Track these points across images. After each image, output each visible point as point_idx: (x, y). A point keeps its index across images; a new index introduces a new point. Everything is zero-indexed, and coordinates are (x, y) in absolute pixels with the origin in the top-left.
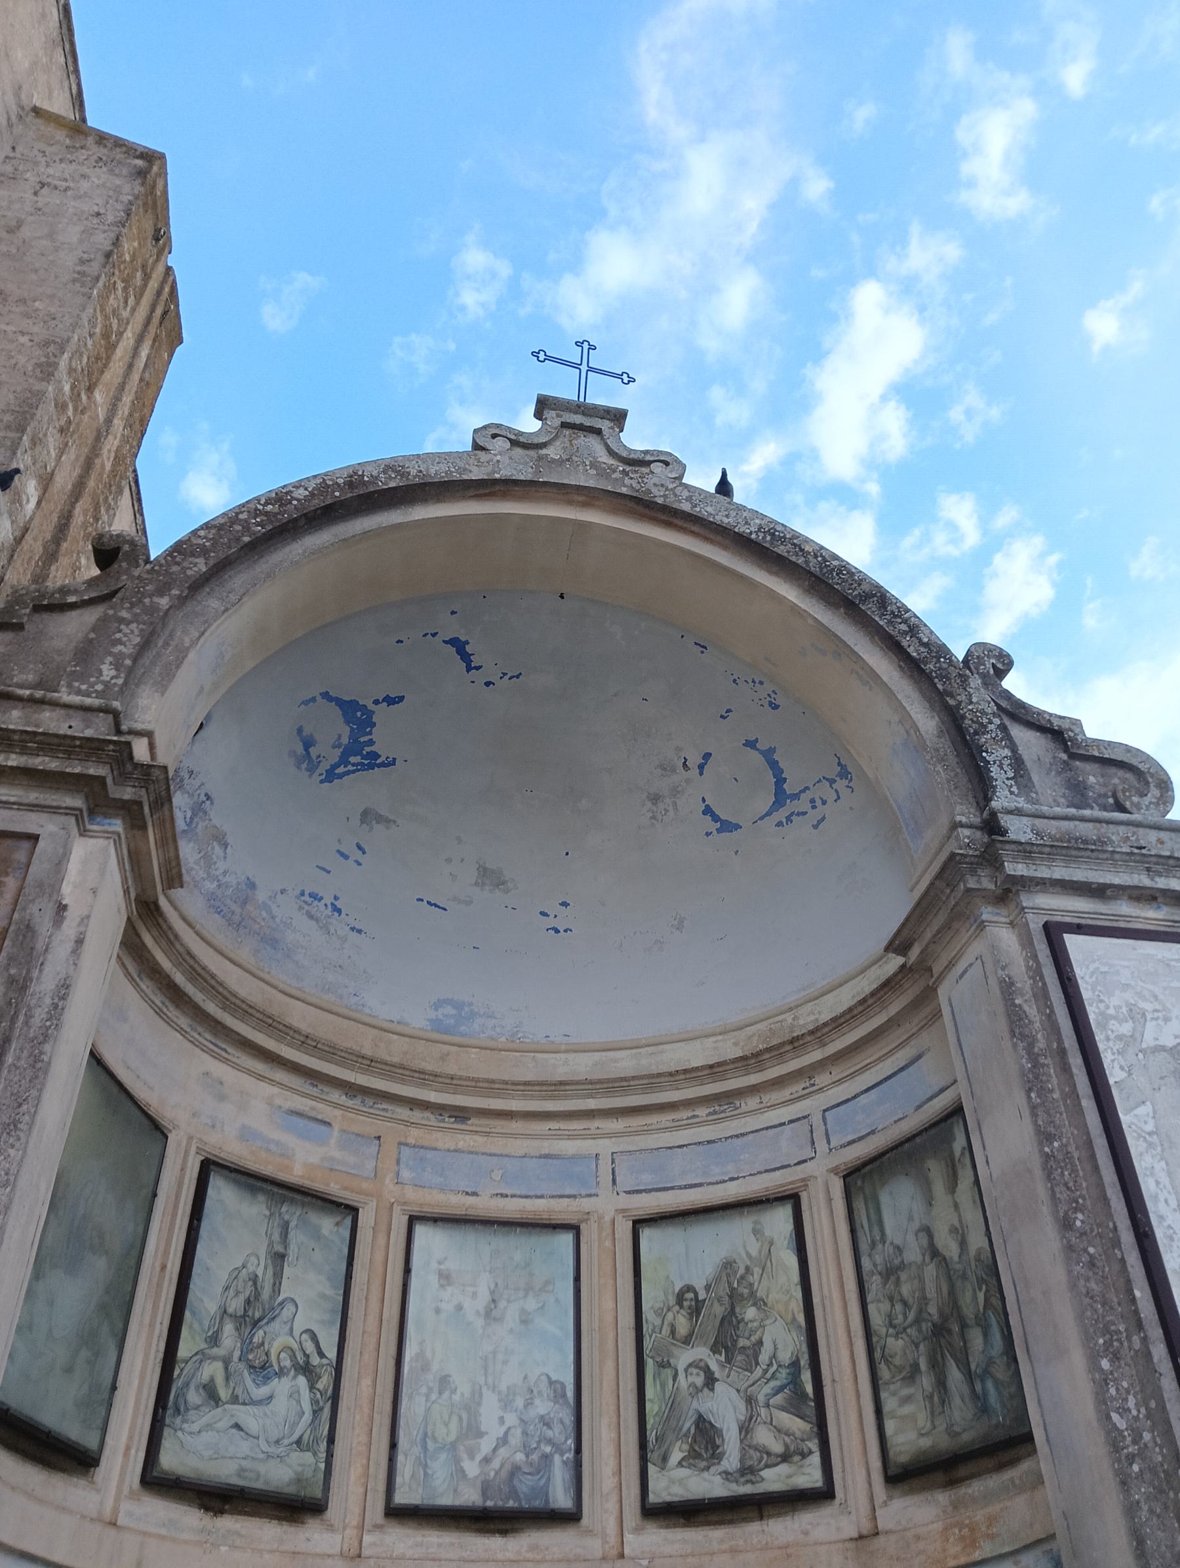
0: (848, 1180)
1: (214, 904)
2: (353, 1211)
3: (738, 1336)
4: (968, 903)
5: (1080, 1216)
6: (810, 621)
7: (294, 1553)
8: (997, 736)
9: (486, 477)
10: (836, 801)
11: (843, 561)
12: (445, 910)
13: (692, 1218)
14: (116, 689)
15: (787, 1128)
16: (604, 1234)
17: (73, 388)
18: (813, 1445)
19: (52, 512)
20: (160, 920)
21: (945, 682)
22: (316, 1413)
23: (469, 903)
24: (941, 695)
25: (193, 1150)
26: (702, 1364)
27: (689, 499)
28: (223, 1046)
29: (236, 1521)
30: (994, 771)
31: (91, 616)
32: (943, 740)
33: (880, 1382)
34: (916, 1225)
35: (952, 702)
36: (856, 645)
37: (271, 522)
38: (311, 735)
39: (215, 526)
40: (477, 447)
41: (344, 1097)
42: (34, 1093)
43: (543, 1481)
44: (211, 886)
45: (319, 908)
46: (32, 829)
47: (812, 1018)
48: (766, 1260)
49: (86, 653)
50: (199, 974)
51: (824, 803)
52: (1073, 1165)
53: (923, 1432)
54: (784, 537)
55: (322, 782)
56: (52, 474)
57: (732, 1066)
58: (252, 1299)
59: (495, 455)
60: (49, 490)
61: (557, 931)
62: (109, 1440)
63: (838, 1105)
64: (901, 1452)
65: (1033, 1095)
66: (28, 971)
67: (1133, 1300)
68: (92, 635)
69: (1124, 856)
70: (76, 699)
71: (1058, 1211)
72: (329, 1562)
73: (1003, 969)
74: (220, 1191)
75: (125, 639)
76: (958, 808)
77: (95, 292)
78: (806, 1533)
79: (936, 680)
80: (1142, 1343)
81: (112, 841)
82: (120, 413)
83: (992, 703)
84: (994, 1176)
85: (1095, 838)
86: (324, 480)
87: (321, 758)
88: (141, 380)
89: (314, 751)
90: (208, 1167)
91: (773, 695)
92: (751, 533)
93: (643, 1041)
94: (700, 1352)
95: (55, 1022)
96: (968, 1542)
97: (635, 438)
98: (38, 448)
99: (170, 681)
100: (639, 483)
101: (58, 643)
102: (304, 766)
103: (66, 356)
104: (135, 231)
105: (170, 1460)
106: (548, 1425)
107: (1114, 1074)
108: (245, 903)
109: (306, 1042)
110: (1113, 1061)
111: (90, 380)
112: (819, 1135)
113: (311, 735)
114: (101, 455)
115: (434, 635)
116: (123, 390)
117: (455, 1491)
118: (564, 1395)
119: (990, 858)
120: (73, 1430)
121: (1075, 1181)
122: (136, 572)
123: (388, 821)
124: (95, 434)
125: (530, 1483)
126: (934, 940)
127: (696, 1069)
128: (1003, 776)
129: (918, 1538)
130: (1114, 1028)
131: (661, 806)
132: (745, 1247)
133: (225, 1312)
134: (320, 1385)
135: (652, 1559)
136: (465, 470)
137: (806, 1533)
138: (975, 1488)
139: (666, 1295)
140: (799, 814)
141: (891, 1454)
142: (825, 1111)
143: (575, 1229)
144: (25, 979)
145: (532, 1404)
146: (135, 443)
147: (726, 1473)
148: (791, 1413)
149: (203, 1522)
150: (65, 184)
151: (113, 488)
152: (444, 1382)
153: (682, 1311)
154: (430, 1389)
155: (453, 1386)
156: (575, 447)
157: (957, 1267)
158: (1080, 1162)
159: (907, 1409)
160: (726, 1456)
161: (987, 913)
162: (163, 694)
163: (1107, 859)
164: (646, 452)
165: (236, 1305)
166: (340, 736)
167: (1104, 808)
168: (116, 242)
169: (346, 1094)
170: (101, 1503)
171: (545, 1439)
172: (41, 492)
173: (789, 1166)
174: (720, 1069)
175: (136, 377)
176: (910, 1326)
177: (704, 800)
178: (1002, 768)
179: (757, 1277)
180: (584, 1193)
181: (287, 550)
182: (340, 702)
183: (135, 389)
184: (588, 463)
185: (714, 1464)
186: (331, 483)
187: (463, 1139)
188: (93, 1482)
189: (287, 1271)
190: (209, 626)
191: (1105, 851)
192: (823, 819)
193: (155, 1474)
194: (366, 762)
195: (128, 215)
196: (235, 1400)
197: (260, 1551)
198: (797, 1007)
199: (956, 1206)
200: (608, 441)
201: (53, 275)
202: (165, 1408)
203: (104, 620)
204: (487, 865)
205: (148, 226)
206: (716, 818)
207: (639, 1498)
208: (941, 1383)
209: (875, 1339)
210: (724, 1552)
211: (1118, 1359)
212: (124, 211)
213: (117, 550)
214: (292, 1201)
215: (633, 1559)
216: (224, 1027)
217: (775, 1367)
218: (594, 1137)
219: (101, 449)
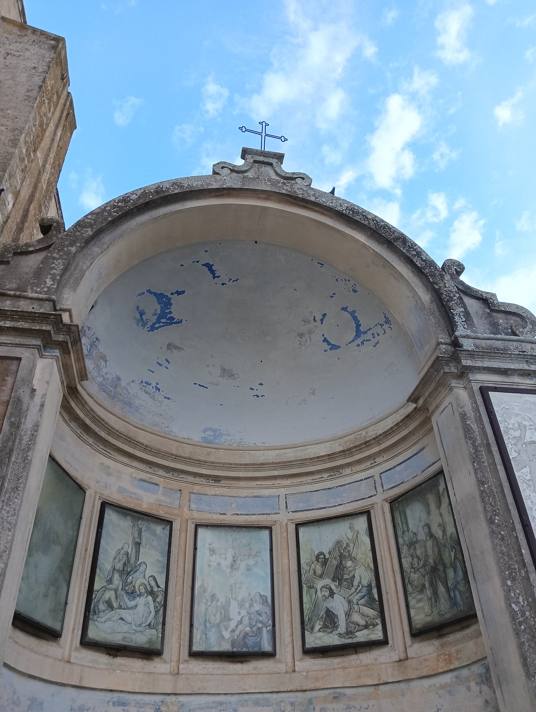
1: (102, 387)
2: (170, 523)
5: (497, 518)
6: (371, 251)
7: (149, 673)
9: (219, 187)
10: (384, 334)
11: (386, 222)
12: (207, 388)
13: (322, 522)
14: (53, 290)
16: (283, 530)
17: (27, 151)
18: (379, 621)
19: (20, 209)
20: (78, 395)
21: (433, 278)
22: (157, 612)
24: (432, 284)
25: (97, 498)
26: (328, 587)
27: (314, 195)
28: (109, 451)
29: (123, 660)
31: (40, 257)
32: (433, 304)
33: (408, 593)
35: (437, 287)
36: (392, 261)
38: (143, 310)
40: (215, 173)
42: (25, 474)
43: (258, 640)
45: (150, 389)
46: (18, 355)
47: (375, 432)
50: (96, 419)
51: (378, 335)
52: (494, 495)
53: (427, 614)
55: (149, 331)
56: (19, 191)
57: (338, 455)
61: (258, 396)
62: (65, 626)
63: (387, 471)
65: (475, 464)
66: (20, 420)
67: (521, 554)
68: (41, 266)
69: (516, 356)
70: (35, 295)
71: (487, 516)
72: (165, 676)
73: (461, 408)
74: (110, 516)
75: (56, 267)
76: (440, 336)
77: (35, 105)
78: (376, 659)
79: (429, 277)
80: (525, 573)
81: (55, 359)
82: (49, 162)
83: (455, 287)
86: (144, 190)
87: (148, 320)
88: (58, 146)
90: (104, 505)
91: (354, 286)
92: (343, 210)
93: (298, 445)
94: (327, 581)
96: (448, 661)
98: (12, 179)
99: (78, 286)
100: (290, 188)
101: (26, 270)
102: (140, 324)
103: (23, 135)
104: (53, 76)
105: (93, 634)
107: (512, 454)
108: (116, 387)
109: (146, 448)
110: (511, 448)
111: (34, 147)
112: (378, 485)
113: (143, 310)
114: (41, 182)
115: (198, 262)
116: (50, 151)
117: (220, 645)
118: (267, 601)
119: (455, 358)
120: (50, 622)
121: (495, 502)
124: (38, 172)
125: (253, 641)
126: (429, 396)
128: (461, 320)
129: (426, 660)
130: (512, 434)
131: (304, 338)
132: (346, 535)
133: (114, 569)
135: (308, 672)
136: (210, 184)
137: (376, 659)
138: (451, 638)
141: (413, 624)
143: (270, 528)
144: (18, 423)
145: (253, 605)
146: (56, 176)
149: (108, 660)
151: (47, 197)
152: (213, 597)
153: (319, 564)
154: (207, 600)
155: (217, 599)
156: (261, 172)
157: (442, 541)
158: (497, 494)
159: (420, 605)
160: (339, 627)
161: (454, 383)
162: (75, 292)
163: (508, 358)
164: (293, 173)
165: (119, 566)
166: (156, 310)
167: (507, 334)
168: (44, 81)
170: (63, 653)
172: (15, 200)
173: (365, 498)
174: (333, 456)
175: (55, 145)
176: (421, 568)
178: (460, 317)
179: (351, 548)
180: (273, 513)
181: (129, 223)
182: (155, 294)
183: (55, 150)
185: (334, 630)
186: (148, 192)
187: (219, 491)
188: (59, 644)
191: (508, 354)
192: (378, 342)
194: (169, 322)
195: (49, 68)
196: (120, 607)
197: (134, 673)
198: (367, 427)
199: (441, 515)
200: (276, 169)
201: (15, 97)
202: (89, 612)
203: (46, 258)
204: (225, 367)
205: (58, 73)
206: (329, 343)
207: (301, 646)
208: (435, 593)
209: (405, 574)
210: (339, 668)
211: (515, 580)
214: (143, 519)
215: (299, 672)
217: (361, 587)
219: (41, 179)
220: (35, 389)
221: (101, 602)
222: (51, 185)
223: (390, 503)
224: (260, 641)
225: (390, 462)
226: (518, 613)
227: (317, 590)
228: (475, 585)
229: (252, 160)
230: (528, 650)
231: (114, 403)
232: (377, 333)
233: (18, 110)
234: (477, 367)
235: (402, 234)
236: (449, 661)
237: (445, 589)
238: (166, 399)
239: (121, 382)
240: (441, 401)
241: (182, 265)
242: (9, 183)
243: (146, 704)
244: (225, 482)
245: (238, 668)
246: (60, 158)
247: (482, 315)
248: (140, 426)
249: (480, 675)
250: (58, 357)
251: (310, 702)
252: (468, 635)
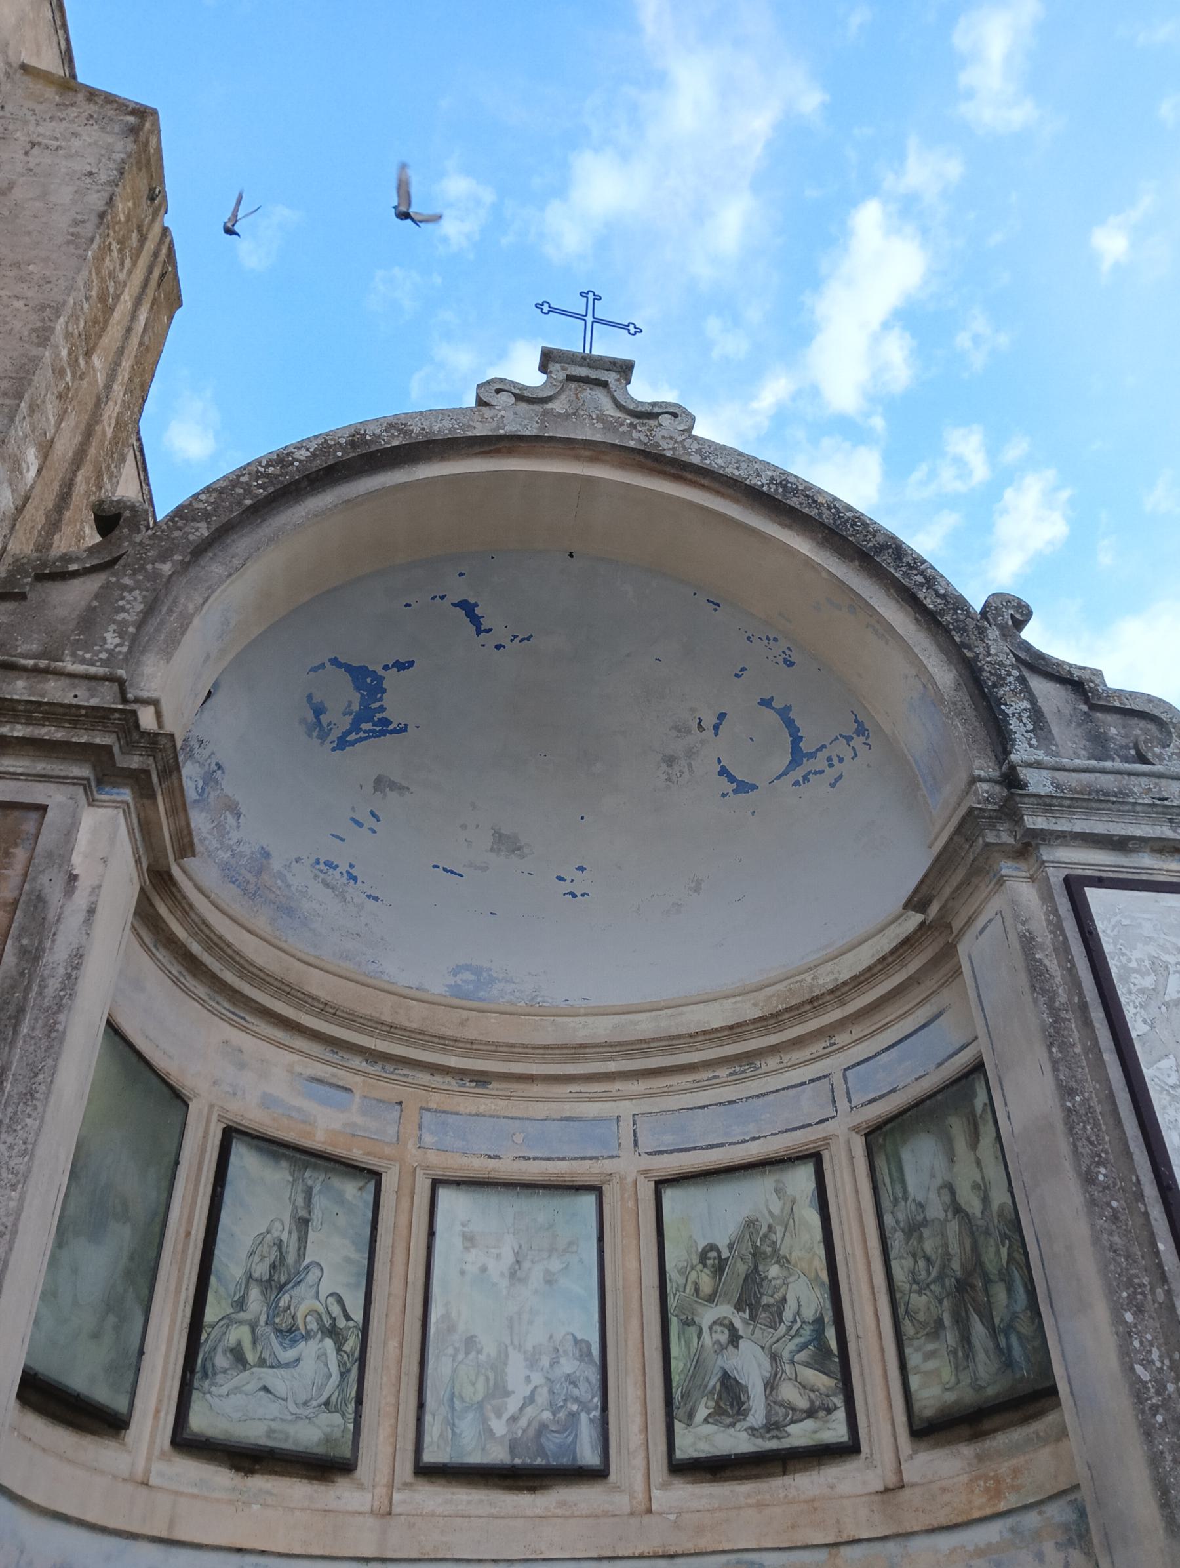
0: (870, 1138)
1: (229, 873)
2: (376, 1176)
3: (762, 1294)
4: (988, 858)
5: (1103, 1170)
6: (824, 575)
7: (325, 1511)
8: (1016, 688)
9: (490, 433)
10: (853, 759)
11: (857, 512)
12: (462, 876)
14: (121, 657)
15: (808, 1087)
16: (626, 1195)
17: (70, 354)
18: (838, 1401)
19: (52, 481)
20: (174, 890)
22: (344, 1375)
23: (484, 869)
24: (959, 647)
25: (215, 1117)
26: (726, 1322)
27: (699, 451)
28: (242, 1015)
29: (267, 1480)
30: (1014, 724)
31: (93, 584)
32: (960, 693)
33: (905, 1337)
34: (938, 1182)
35: (969, 654)
37: (273, 484)
39: (215, 490)
40: (481, 402)
41: (364, 1064)
42: (50, 1062)
43: (570, 1439)
44: (225, 856)
45: (334, 876)
47: (832, 977)
49: (89, 622)
50: (216, 944)
51: (841, 760)
52: (1095, 1119)
53: (947, 1386)
54: (797, 489)
55: (333, 749)
56: (52, 441)
57: (751, 1027)
58: (277, 1263)
59: (500, 410)
60: (49, 457)
61: (574, 895)
63: (859, 1064)
64: (925, 1407)
65: (1054, 1050)
66: (40, 942)
67: (1157, 1253)
68: (95, 603)
70: (80, 668)
71: (1080, 1166)
73: (1023, 923)
74: (243, 1158)
75: (128, 606)
76: (977, 763)
77: (90, 253)
78: (832, 1487)
79: (953, 633)
81: (121, 810)
82: (120, 378)
83: (1011, 655)
84: (1016, 1132)
85: (1116, 790)
86: (325, 440)
88: (141, 344)
89: (324, 719)
90: (230, 1134)
91: (788, 652)
92: (763, 485)
93: (663, 1004)
94: (725, 1310)
95: (69, 992)
97: (641, 391)
98: (37, 416)
99: (175, 649)
100: (647, 436)
101: (61, 612)
102: (315, 734)
103: (62, 320)
104: (129, 191)
105: (200, 1422)
106: (574, 1384)
107: (1137, 1028)
108: (259, 873)
109: (325, 1009)
110: (1135, 1014)
112: (840, 1095)
114: (102, 421)
115: (442, 598)
116: (122, 354)
117: (483, 1449)
118: (589, 1354)
119: (1009, 812)
120: (103, 1395)
121: (1098, 1136)
122: (138, 538)
123: (401, 789)
124: (94, 400)
125: (557, 1441)
126: (952, 897)
127: (717, 1030)
128: (1023, 729)
129: (944, 1490)
131: (676, 768)
132: (767, 1206)
133: (251, 1276)
134: (347, 1347)
136: (469, 426)
137: (832, 1487)
138: (1000, 1441)
139: (689, 1254)
140: (816, 773)
142: (845, 1070)
143: (598, 1190)
144: (37, 949)
145: (558, 1363)
146: (136, 410)
147: (753, 1429)
148: (818, 1370)
150: (56, 143)
151: (115, 456)
152: (470, 1342)
153: (705, 1270)
154: (457, 1350)
155: (479, 1346)
157: (980, 1223)
159: (931, 1365)
160: (752, 1412)
161: (1007, 868)
163: (1128, 811)
164: (654, 404)
165: (261, 1270)
166: (350, 703)
167: (1126, 759)
168: (110, 202)
169: (367, 1061)
171: (572, 1397)
175: (135, 341)
176: (934, 1282)
177: (719, 761)
178: (1021, 721)
179: (779, 1235)
182: (349, 668)
183: (134, 354)
184: (594, 417)
185: (739, 1421)
188: (124, 1444)
189: (311, 1235)
190: (213, 592)
191: (1128, 803)
192: (841, 777)
193: (185, 1436)
194: (378, 729)
195: (122, 174)
196: (262, 1363)
198: (816, 966)
199: (978, 1162)
200: (615, 394)
202: (193, 1372)
203: (106, 586)
204: (503, 831)
205: (143, 185)
206: (732, 779)
209: (898, 1295)
210: (750, 1506)
212: (116, 169)
213: (118, 516)
214: (315, 1167)
215: (661, 1514)
216: (243, 996)
217: (799, 1323)
218: (615, 1099)
219: (101, 415)
220: (76, 876)
221: (219, 1350)
222: (125, 428)
223: (866, 1135)
224: (574, 1442)
225: (866, 1043)
226: (1150, 1385)
227: (701, 1329)
228: (1052, 1321)
229: (562, 376)
230: (1171, 1469)
231: (255, 909)
232: (838, 757)
233: (50, 264)
234: (1059, 834)
235: (894, 538)
236: (996, 1493)
237: (988, 1329)
238: (371, 901)
239: (271, 861)
240: (979, 907)
241: (407, 605)
242: (30, 423)
244: (498, 1086)
245: (524, 1502)
246: (144, 370)
247: (1071, 716)
248: (311, 960)
249: (1066, 1528)
250: (128, 804)
252: (1038, 1436)
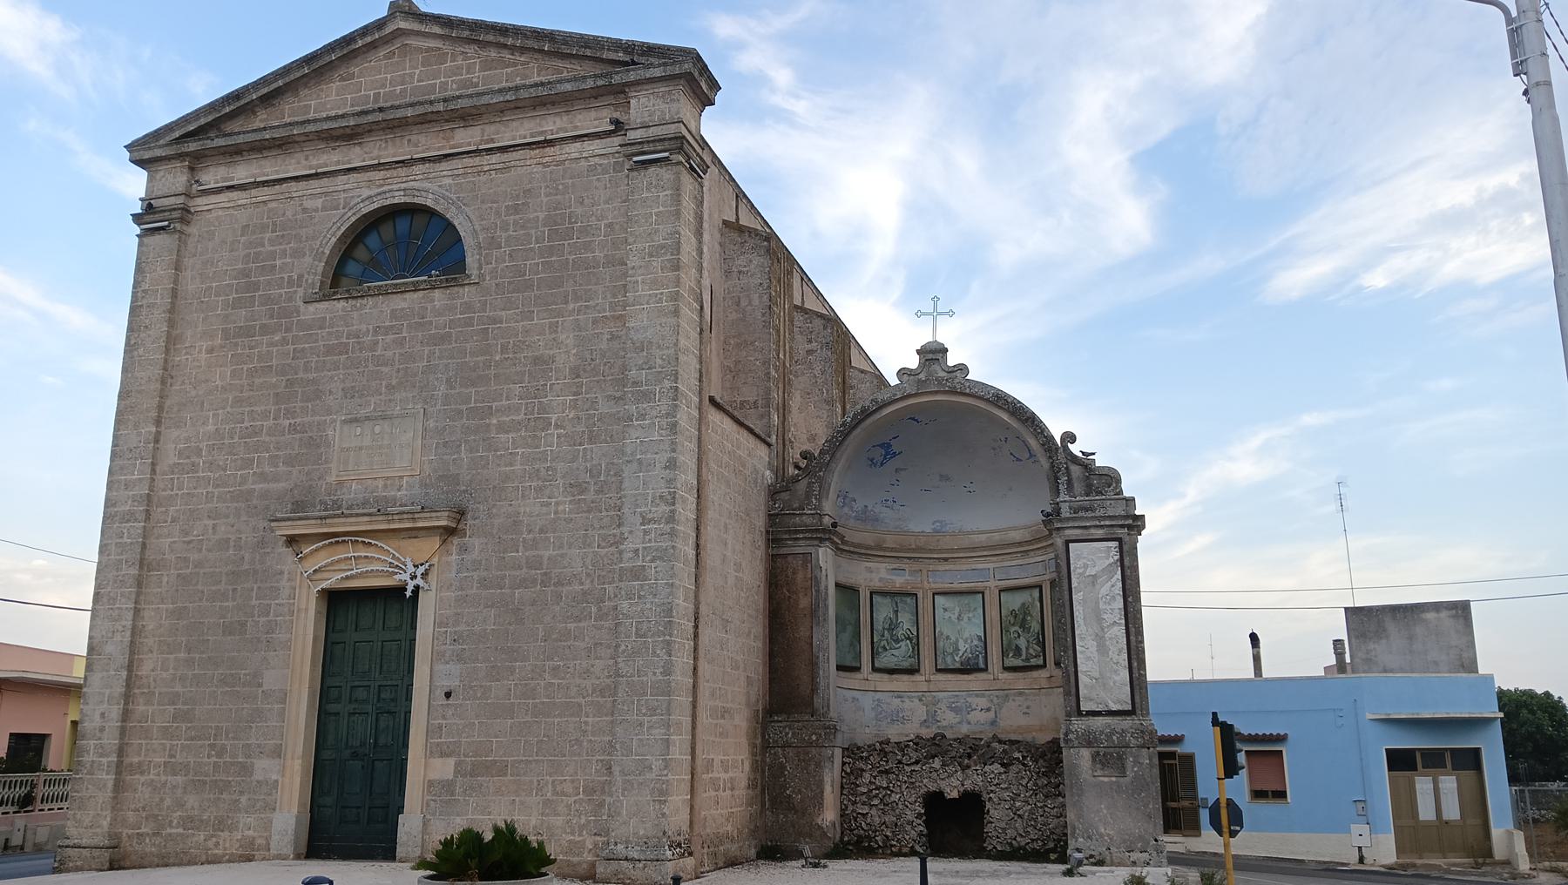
22: (913, 649)
48: (1033, 604)
70: (810, 512)
94: (1017, 628)
120: (854, 664)
123: (905, 469)
152: (948, 637)
165: (887, 626)
196: (891, 649)
243: (913, 697)
251: (1007, 696)
